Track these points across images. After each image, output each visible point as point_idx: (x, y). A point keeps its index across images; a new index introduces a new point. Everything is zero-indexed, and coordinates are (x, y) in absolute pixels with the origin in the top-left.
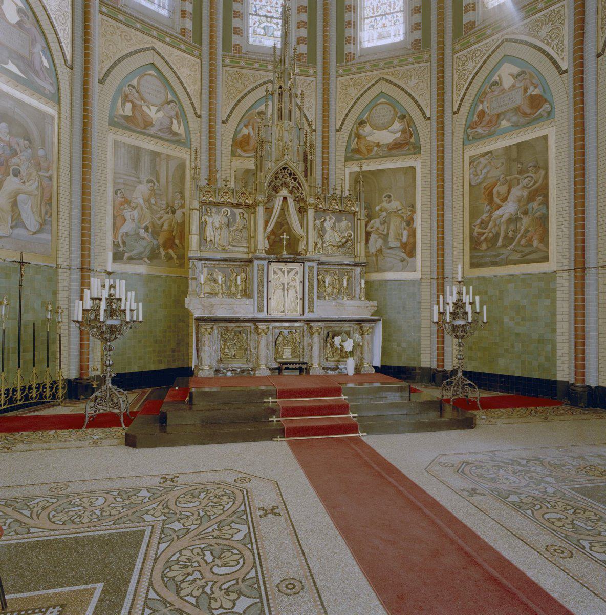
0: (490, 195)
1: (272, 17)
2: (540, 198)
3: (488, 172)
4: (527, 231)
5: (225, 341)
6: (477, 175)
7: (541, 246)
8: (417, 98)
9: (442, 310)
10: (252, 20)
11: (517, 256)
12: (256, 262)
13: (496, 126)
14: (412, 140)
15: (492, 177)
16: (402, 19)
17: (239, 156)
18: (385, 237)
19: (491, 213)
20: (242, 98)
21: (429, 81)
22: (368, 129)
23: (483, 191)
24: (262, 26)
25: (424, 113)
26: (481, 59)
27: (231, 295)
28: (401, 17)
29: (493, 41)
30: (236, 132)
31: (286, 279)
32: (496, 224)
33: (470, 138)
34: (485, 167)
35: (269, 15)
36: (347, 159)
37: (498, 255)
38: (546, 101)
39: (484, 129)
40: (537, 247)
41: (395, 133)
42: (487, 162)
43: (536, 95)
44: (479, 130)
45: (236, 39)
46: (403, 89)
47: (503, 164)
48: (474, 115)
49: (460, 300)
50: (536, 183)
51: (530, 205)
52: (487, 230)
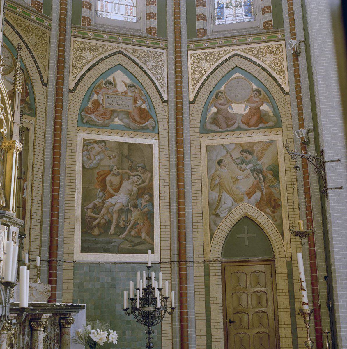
0: (104, 181)
2: (147, 196)
3: (101, 160)
4: (136, 223)
6: (91, 159)
7: (148, 238)
8: (36, 58)
9: (132, 296)
11: (127, 246)
13: (111, 120)
15: (105, 166)
21: (48, 47)
23: (96, 176)
26: (99, 55)
29: (110, 46)
32: (108, 211)
33: (85, 121)
34: (99, 153)
37: (109, 243)
38: (152, 117)
39: (98, 118)
40: (144, 239)
42: (100, 150)
43: (144, 109)
44: (93, 117)
47: (115, 157)
48: (89, 101)
49: (149, 286)
50: (143, 182)
51: (139, 201)
52: (99, 216)
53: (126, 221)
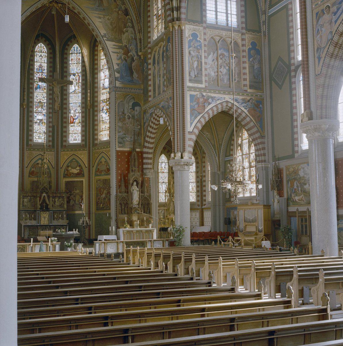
1: (41, 133)
5: (30, 231)
10: (35, 134)
12: (37, 212)
14: (82, 173)
16: (80, 136)
17: (31, 177)
18: (75, 201)
19: (100, 196)
20: (32, 160)
22: (70, 168)
24: (38, 136)
25: (85, 166)
27: (30, 220)
28: (80, 135)
30: (30, 170)
31: (45, 215)
35: (40, 132)
36: (64, 177)
41: (77, 170)
45: (30, 143)
46: (80, 158)
53: (105, 201)
